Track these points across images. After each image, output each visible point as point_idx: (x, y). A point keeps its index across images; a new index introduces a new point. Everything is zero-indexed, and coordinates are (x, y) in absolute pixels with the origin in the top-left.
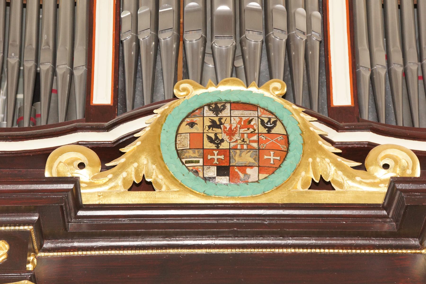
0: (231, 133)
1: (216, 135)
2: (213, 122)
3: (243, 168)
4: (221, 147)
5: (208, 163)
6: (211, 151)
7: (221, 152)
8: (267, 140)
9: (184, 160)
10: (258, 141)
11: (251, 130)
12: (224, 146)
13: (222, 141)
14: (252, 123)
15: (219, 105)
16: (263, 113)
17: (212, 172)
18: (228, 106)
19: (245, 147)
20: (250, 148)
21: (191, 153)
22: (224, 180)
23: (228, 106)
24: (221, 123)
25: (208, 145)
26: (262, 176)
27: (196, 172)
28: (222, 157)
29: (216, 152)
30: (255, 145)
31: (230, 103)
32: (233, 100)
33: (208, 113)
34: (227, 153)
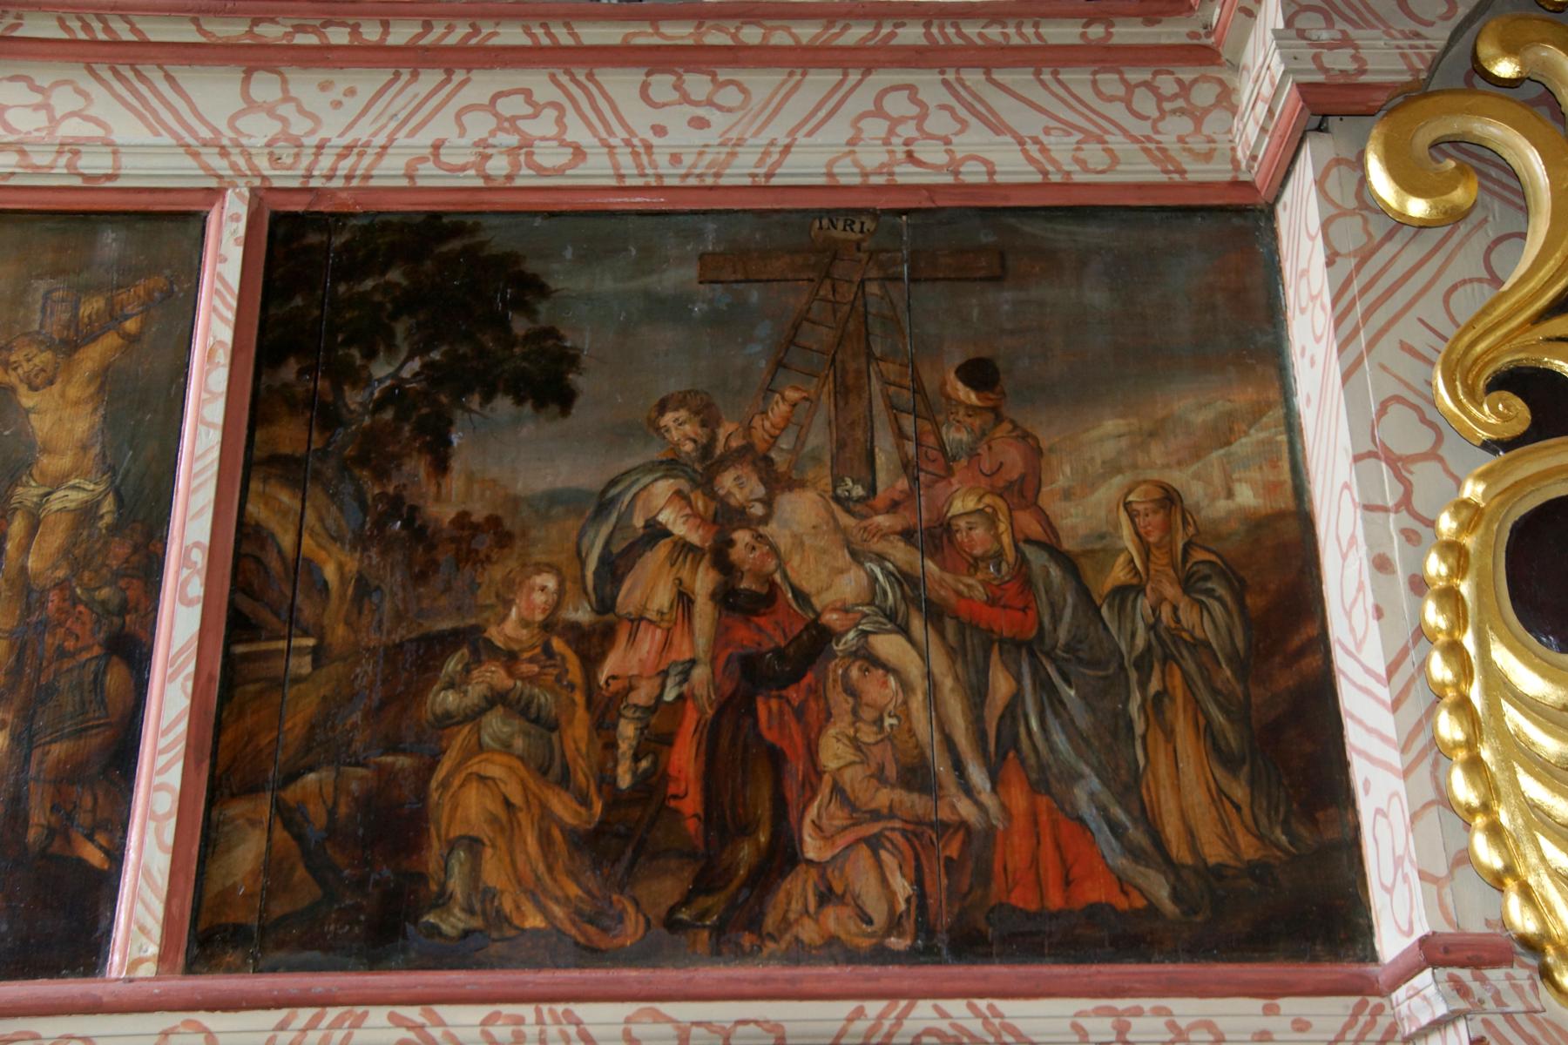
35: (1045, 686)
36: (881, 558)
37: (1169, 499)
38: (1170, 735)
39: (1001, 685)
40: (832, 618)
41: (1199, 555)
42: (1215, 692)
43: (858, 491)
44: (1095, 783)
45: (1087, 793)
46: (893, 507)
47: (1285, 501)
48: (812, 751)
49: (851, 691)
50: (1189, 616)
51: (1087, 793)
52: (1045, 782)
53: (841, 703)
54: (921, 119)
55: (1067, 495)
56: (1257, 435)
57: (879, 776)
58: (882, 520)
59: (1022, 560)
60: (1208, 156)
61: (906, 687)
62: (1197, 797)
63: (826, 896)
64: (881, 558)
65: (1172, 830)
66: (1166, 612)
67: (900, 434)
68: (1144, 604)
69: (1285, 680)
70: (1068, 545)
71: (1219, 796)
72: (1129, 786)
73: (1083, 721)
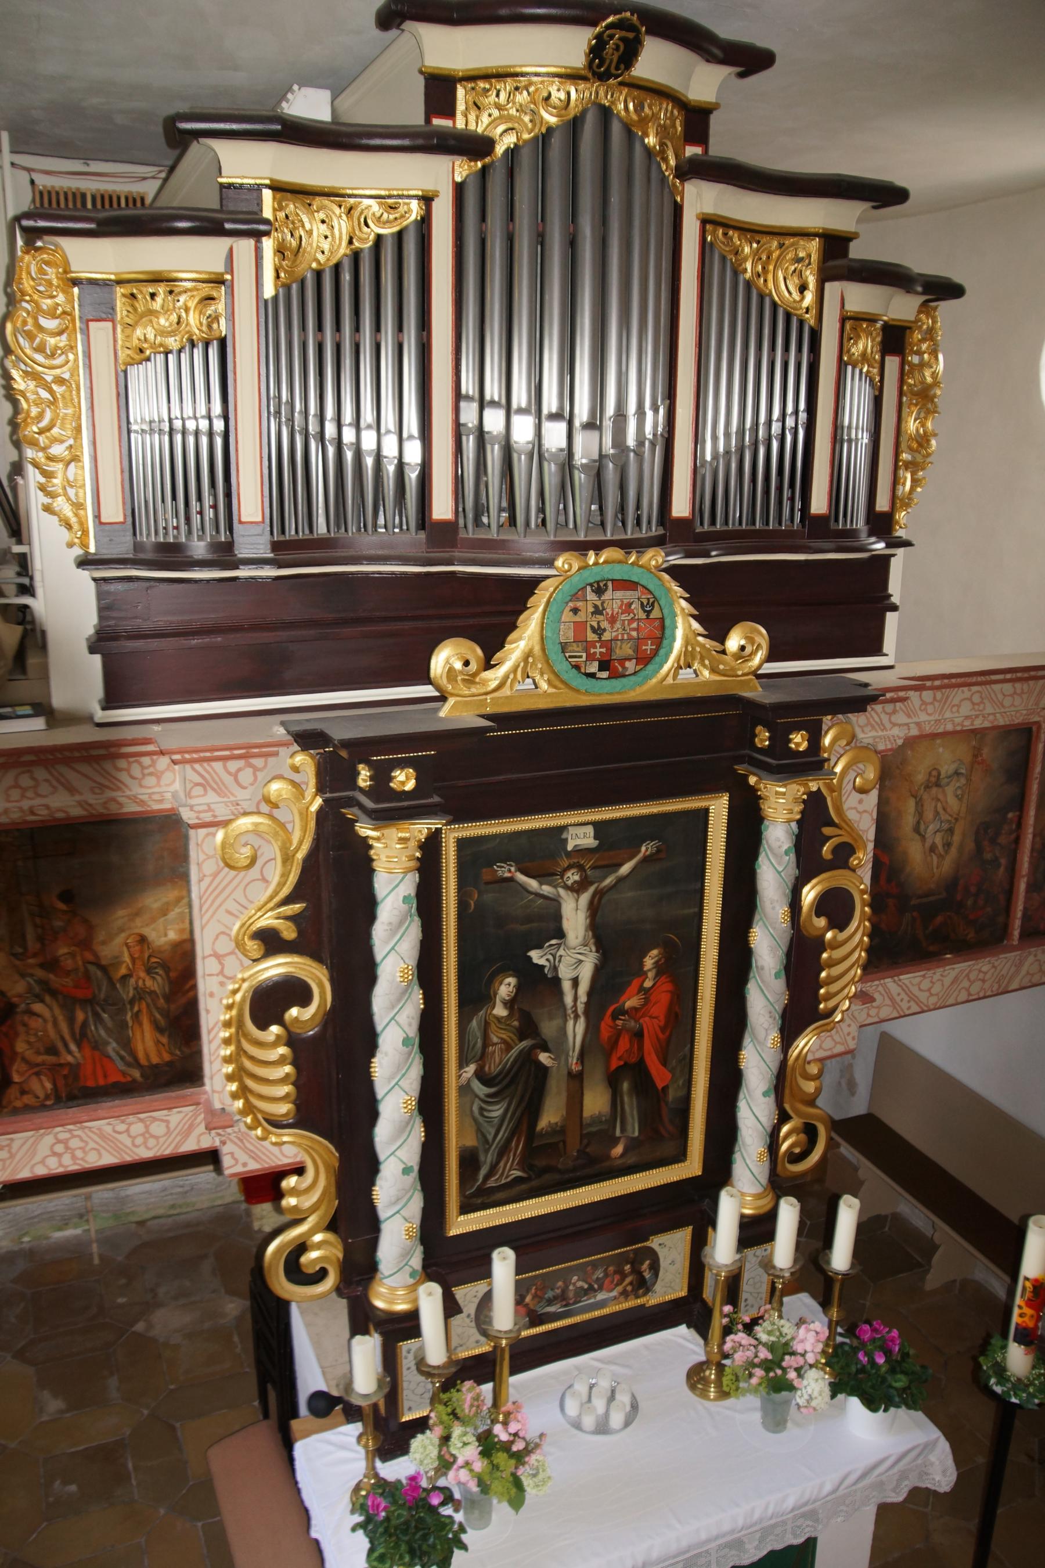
0: (613, 620)
1: (598, 622)
2: (596, 606)
3: (622, 661)
4: (603, 639)
5: (590, 657)
6: (593, 644)
7: (603, 644)
8: (646, 628)
9: (567, 655)
10: (637, 629)
11: (632, 615)
12: (607, 636)
13: (604, 630)
14: (633, 607)
15: (601, 585)
16: (643, 593)
17: (593, 667)
18: (610, 584)
19: (626, 637)
20: (631, 638)
21: (575, 647)
22: (605, 674)
23: (610, 584)
24: (604, 609)
25: (591, 636)
26: (638, 668)
27: (577, 667)
28: (603, 650)
29: (598, 645)
30: (634, 634)
31: (613, 580)
32: (615, 578)
33: (591, 596)
34: (608, 645)
35: (97, 1016)
36: (32, 975)
37: (143, 940)
38: (141, 1024)
39: (80, 1016)
40: (15, 1000)
41: (154, 960)
42: (157, 1008)
43: (20, 950)
44: (114, 1045)
45: (112, 1047)
46: (35, 955)
47: (186, 936)
48: (12, 1047)
49: (25, 1025)
50: (149, 983)
51: (112, 1047)
52: (97, 1046)
53: (21, 1029)
54: (35, 787)
55: (104, 943)
56: (177, 910)
57: (38, 1053)
58: (31, 961)
59: (87, 971)
60: (161, 801)
61: (45, 1021)
62: (150, 1043)
63: (23, 1092)
64: (32, 975)
65: (141, 1055)
66: (140, 983)
67: (36, 926)
68: (132, 981)
69: (183, 1000)
70: (104, 962)
71: (158, 1043)
72: (126, 1044)
73: (110, 1023)
